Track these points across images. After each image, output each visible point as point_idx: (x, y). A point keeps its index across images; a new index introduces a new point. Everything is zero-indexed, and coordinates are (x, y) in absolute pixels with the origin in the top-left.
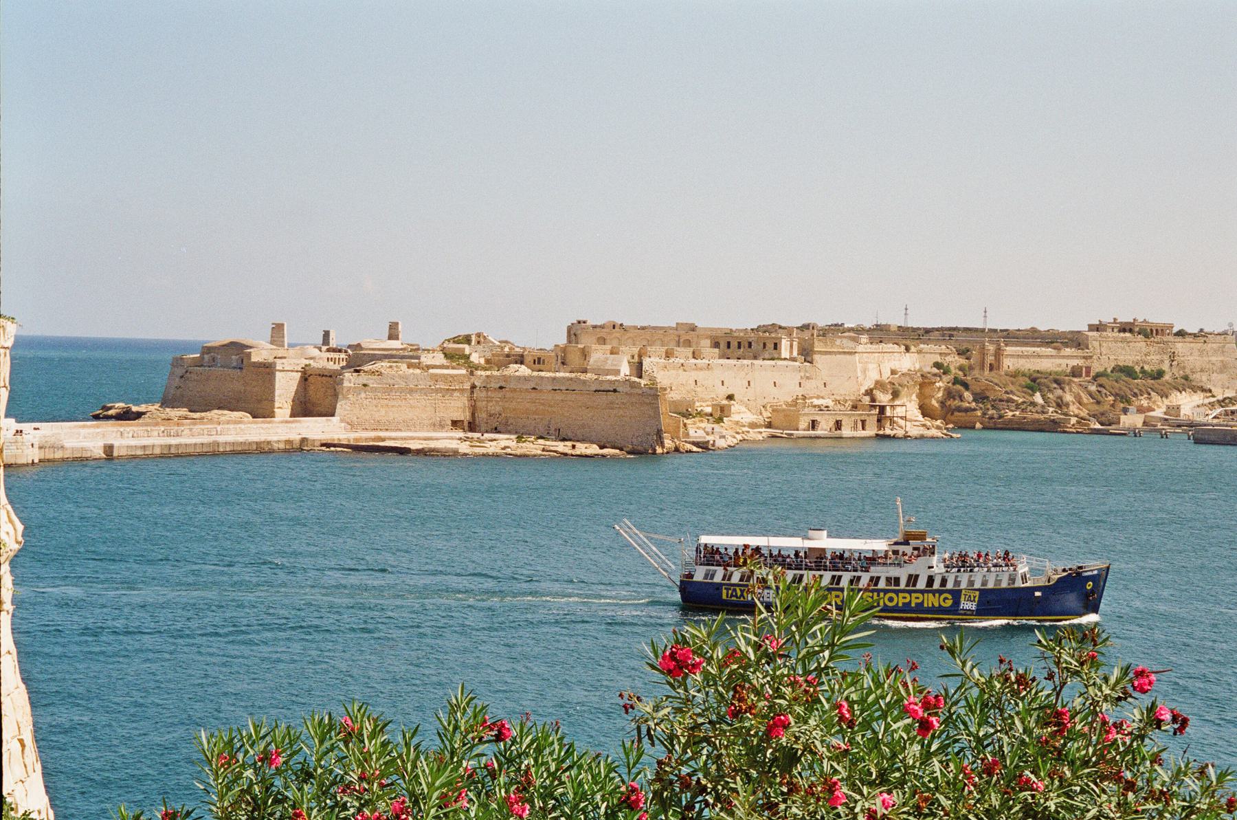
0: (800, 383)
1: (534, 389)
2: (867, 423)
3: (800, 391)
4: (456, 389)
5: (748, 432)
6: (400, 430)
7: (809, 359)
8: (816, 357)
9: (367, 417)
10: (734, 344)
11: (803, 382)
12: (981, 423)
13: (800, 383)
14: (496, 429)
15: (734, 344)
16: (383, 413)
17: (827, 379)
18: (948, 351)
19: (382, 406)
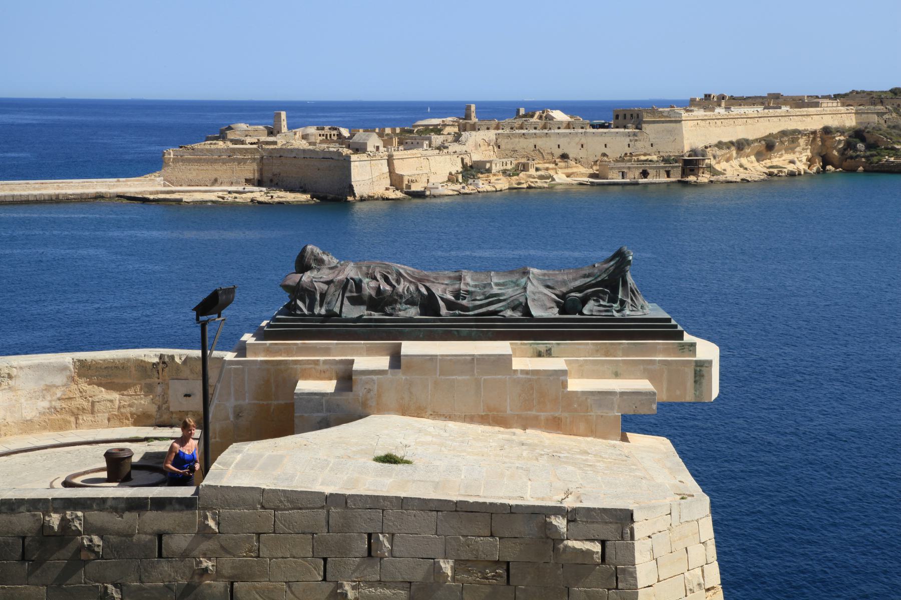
0: (629, 146)
1: (295, 157)
2: (672, 172)
3: (628, 151)
4: (249, 158)
5: (536, 182)
6: (207, 186)
7: (639, 126)
8: (644, 125)
9: (183, 177)
10: (628, 116)
11: (632, 144)
12: (863, 167)
13: (629, 145)
14: (277, 184)
15: (628, 116)
16: (194, 173)
17: (652, 141)
18: (885, 111)
19: (194, 170)
